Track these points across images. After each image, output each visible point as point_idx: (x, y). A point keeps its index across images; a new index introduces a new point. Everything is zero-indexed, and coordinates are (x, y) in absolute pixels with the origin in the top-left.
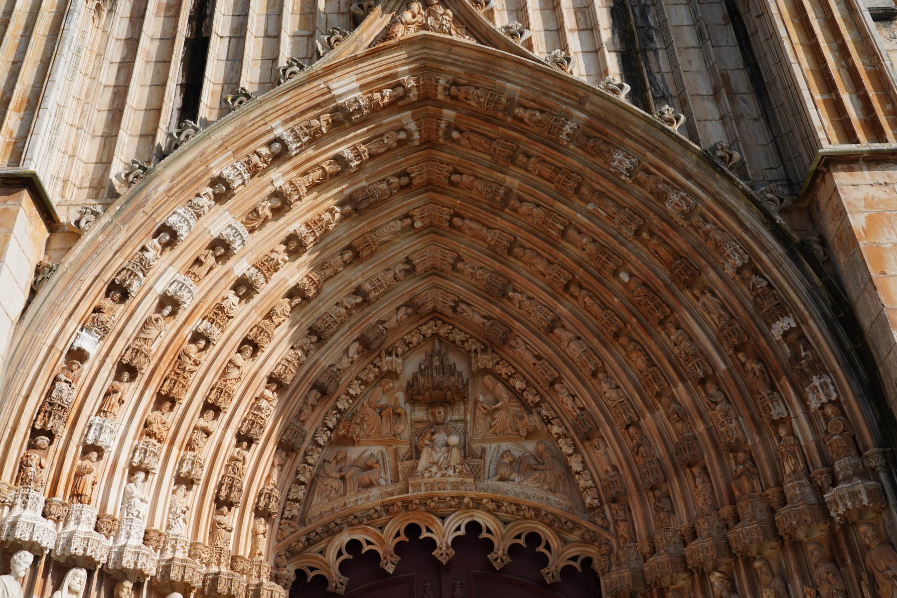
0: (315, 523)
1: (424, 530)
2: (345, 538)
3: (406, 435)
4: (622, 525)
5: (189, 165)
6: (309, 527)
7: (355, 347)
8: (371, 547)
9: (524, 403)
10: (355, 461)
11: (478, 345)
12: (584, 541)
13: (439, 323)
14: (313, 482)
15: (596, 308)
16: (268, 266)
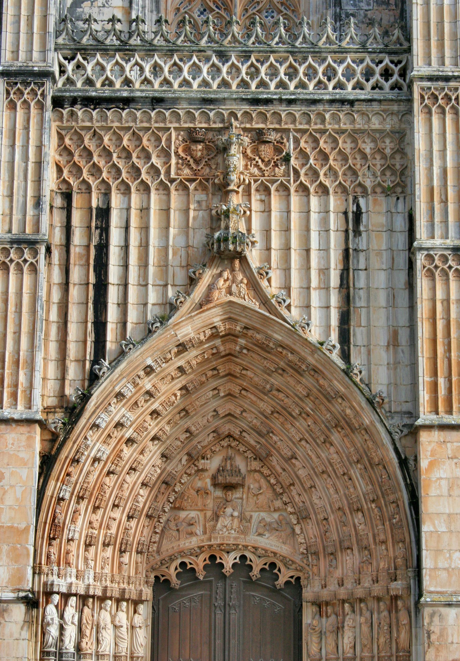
0: (165, 555)
1: (218, 559)
2: (179, 561)
3: (211, 506)
4: (315, 567)
5: (105, 388)
6: (162, 557)
7: (185, 458)
8: (191, 566)
9: (274, 490)
10: (184, 519)
11: (252, 455)
12: (296, 570)
13: (231, 439)
14: (162, 530)
15: (313, 457)
16: (141, 429)
